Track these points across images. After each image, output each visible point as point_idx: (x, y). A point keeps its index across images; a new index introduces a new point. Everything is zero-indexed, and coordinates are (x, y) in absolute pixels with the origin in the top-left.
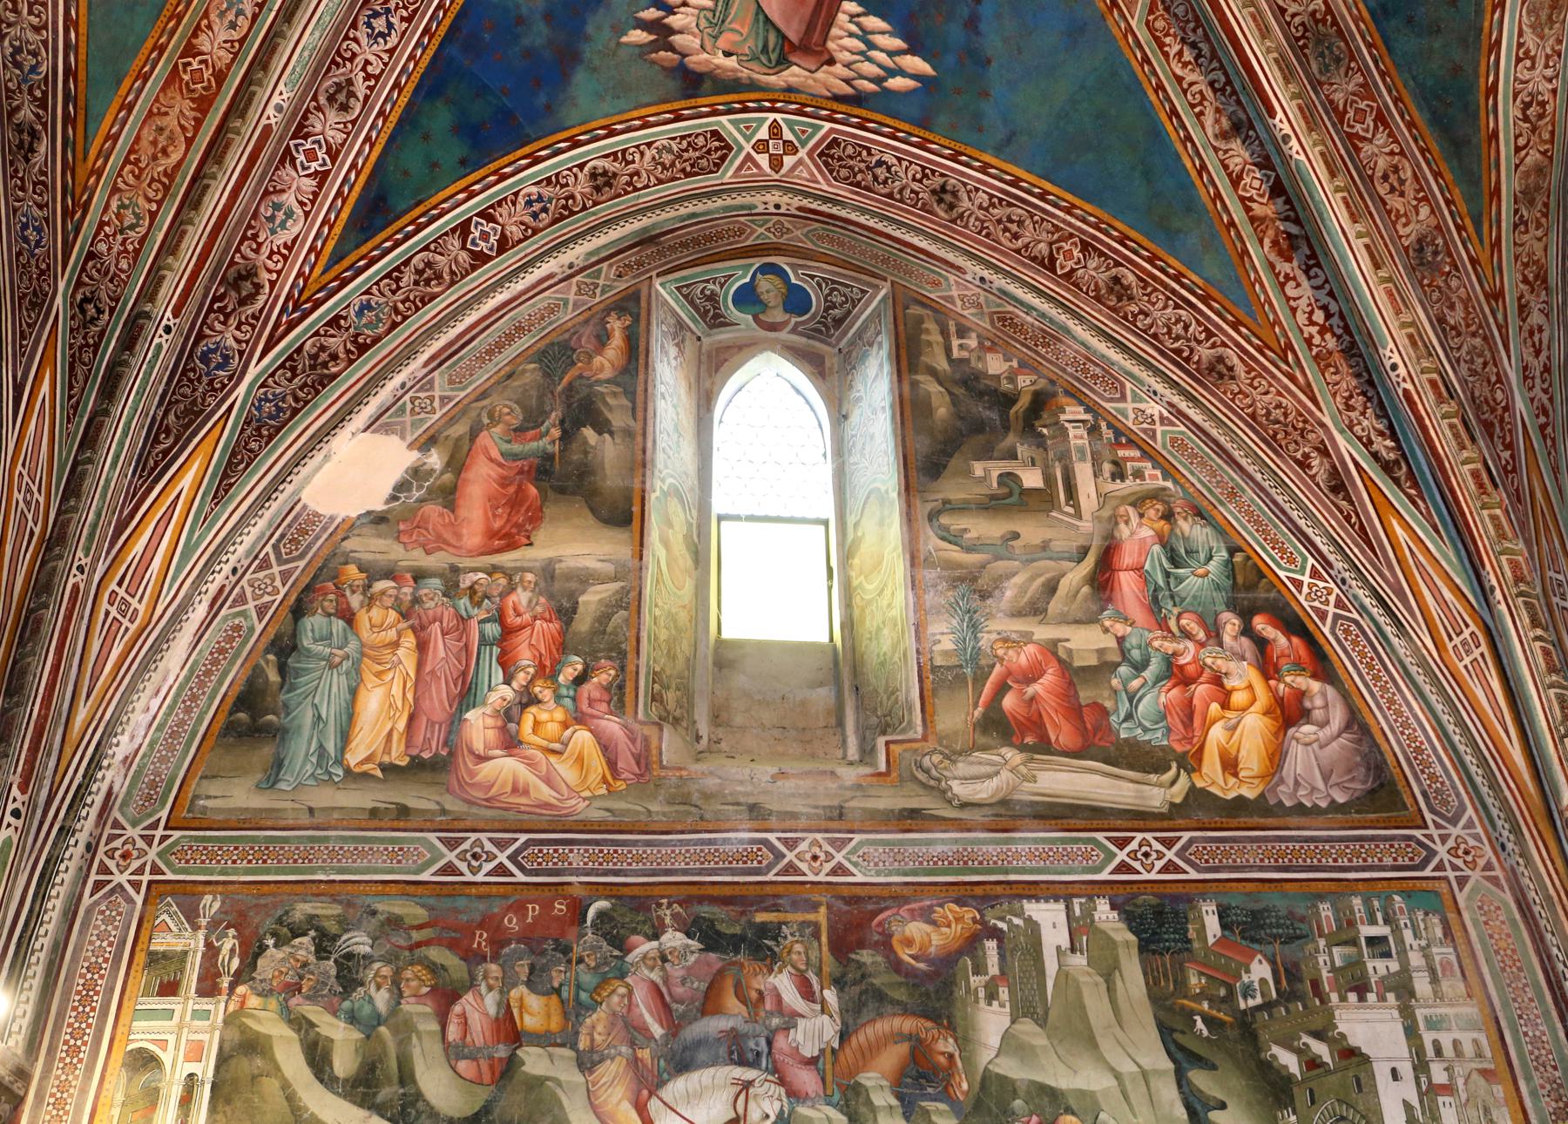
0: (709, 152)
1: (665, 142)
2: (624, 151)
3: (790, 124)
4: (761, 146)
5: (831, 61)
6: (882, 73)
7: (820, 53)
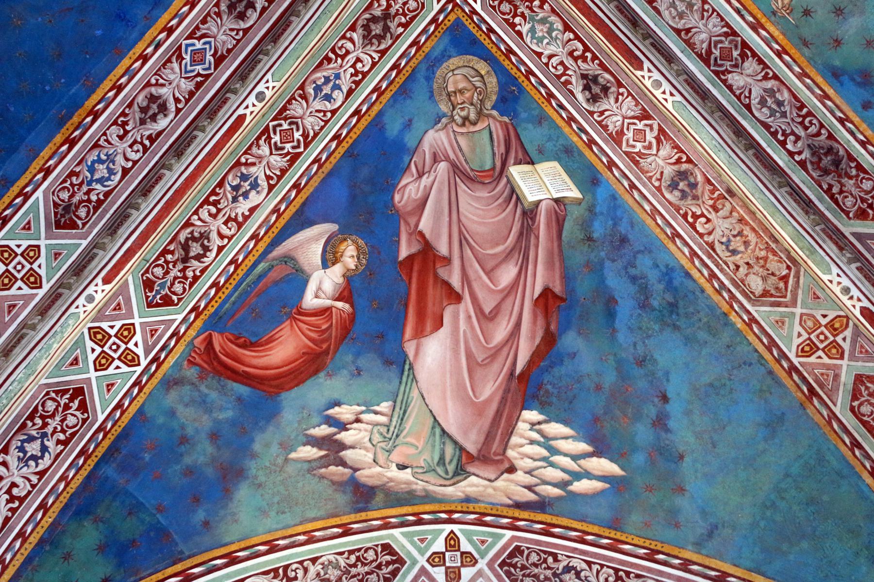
0: (379, 567)
1: (331, 558)
2: (286, 568)
3: (468, 535)
4: (437, 559)
5: (512, 470)
6: (566, 477)
7: (500, 462)
